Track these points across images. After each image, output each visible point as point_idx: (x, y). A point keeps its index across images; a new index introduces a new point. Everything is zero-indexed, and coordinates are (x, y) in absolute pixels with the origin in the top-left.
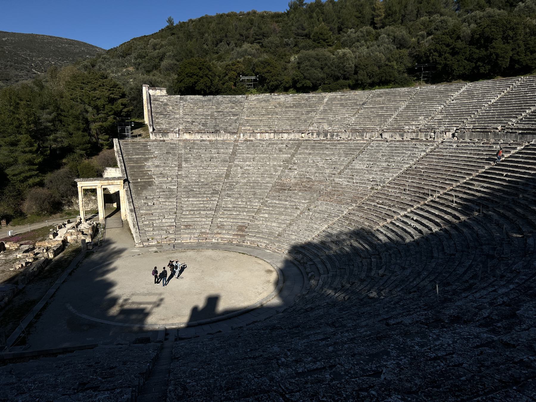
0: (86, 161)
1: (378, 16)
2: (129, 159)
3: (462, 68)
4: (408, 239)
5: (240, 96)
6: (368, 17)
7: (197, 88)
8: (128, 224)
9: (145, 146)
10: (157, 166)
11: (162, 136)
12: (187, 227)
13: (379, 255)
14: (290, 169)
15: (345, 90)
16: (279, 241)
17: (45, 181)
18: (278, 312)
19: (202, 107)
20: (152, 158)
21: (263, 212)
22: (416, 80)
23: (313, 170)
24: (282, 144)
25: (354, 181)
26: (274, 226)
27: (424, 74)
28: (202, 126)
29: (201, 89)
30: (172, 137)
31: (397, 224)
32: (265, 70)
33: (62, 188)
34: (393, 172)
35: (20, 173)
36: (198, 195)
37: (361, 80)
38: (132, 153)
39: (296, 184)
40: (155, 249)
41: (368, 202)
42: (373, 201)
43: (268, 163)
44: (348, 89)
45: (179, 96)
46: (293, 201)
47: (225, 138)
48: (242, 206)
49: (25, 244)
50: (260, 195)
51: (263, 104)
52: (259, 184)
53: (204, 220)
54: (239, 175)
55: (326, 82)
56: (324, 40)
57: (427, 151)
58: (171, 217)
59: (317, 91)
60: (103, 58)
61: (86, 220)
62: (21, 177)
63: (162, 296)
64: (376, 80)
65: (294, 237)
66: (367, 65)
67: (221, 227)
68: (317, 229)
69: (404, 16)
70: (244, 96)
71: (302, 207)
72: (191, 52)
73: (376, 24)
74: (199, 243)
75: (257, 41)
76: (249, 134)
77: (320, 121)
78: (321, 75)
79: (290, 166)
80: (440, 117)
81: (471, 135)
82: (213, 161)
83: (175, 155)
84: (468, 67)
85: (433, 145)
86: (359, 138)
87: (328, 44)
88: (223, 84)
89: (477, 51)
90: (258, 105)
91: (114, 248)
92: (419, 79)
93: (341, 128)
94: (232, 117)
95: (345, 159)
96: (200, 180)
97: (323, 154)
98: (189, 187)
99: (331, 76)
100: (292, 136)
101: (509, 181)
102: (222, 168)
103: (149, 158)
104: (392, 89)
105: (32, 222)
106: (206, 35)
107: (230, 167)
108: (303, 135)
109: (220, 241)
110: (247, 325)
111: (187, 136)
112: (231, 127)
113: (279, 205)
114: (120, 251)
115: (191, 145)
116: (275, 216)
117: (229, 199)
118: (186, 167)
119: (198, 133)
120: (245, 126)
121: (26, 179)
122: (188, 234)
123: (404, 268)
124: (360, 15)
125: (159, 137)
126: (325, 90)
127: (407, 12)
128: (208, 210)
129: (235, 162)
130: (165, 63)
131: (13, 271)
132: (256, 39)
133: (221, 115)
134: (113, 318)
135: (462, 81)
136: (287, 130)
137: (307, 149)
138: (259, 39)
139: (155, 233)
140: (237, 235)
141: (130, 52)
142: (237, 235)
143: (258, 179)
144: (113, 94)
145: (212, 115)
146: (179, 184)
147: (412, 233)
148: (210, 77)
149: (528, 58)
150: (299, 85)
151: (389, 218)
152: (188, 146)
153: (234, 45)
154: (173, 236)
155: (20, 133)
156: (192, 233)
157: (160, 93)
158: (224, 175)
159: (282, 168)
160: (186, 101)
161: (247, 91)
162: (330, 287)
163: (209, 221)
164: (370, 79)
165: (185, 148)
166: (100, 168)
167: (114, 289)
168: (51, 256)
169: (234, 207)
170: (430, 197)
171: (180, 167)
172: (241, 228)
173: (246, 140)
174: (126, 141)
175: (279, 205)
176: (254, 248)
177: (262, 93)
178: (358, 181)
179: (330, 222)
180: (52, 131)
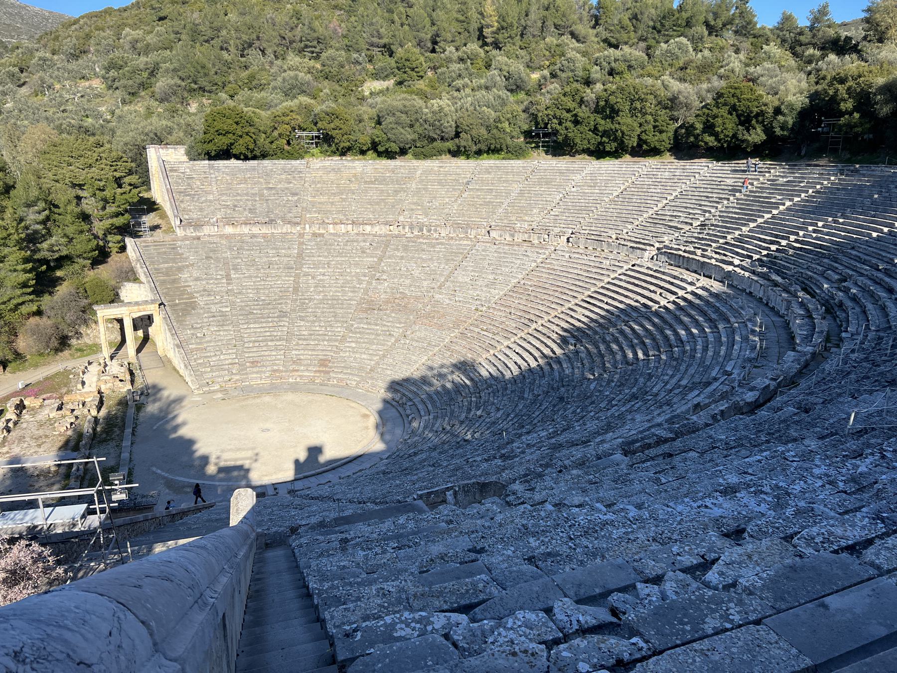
0: (91, 274)
1: (488, 26)
2: (156, 269)
3: (586, 142)
4: (508, 375)
5: (298, 162)
6: (474, 26)
7: (234, 151)
8: (170, 361)
9: (173, 248)
10: (197, 279)
11: (195, 231)
12: (254, 363)
13: (479, 393)
14: (378, 279)
15: (443, 156)
16: (372, 378)
17: (43, 308)
18: (382, 459)
19: (245, 181)
20: (187, 266)
21: (348, 340)
22: (535, 147)
23: (408, 282)
24: (364, 241)
25: (457, 299)
26: (364, 359)
27: (543, 142)
28: (249, 213)
29: (241, 153)
30: (207, 230)
31: (500, 357)
32: (332, 125)
33: (70, 317)
34: (499, 289)
35: (9, 301)
36: (260, 320)
37: (465, 147)
38: (158, 261)
39: (387, 302)
40: (220, 395)
41: (472, 328)
42: (477, 327)
43: (349, 271)
44: (448, 156)
45: (207, 162)
46: (385, 325)
47: (284, 230)
48: (321, 332)
49: (48, 398)
50: (343, 317)
51: (332, 176)
52: (340, 301)
53: (274, 353)
54: (312, 289)
55: (418, 145)
56: (413, 70)
57: (539, 261)
58: (230, 351)
59: (407, 156)
60: (40, 59)
61: (112, 358)
62: (11, 305)
63: (256, 451)
64: (483, 147)
65: (389, 372)
66: (471, 124)
67: (297, 362)
68: (416, 362)
69: (525, 28)
70: (303, 162)
71: (397, 333)
72: (203, 67)
73: (486, 38)
74: (272, 384)
75: (308, 50)
76: (318, 226)
77: (414, 207)
78: (410, 137)
79: (378, 275)
80: (556, 211)
81: (586, 243)
82: (273, 268)
83: (217, 260)
84: (593, 141)
85: (545, 254)
86: (462, 236)
87: (418, 74)
88: (272, 142)
89: (603, 122)
90: (325, 178)
91: (168, 397)
92: (537, 147)
93: (439, 220)
94: (290, 198)
95: (446, 267)
96: (259, 298)
97: (419, 258)
98: (247, 308)
99: (425, 137)
100: (376, 229)
101: (607, 311)
102: (287, 278)
103: (183, 266)
104: (504, 162)
105: (36, 366)
106: (224, 32)
107: (297, 276)
108: (391, 227)
109: (298, 380)
110: (354, 474)
111: (229, 230)
112: (290, 215)
113: (368, 331)
114: (179, 400)
115: (239, 244)
116: (364, 345)
117: (302, 323)
118: (238, 278)
119: (246, 224)
120: (310, 213)
121: (17, 306)
122: (257, 373)
123: (498, 409)
124: (462, 18)
125: (190, 232)
126: (417, 156)
127: (529, 23)
128: (277, 340)
129: (304, 270)
130: (162, 83)
131: (60, 435)
132: (306, 46)
133: (274, 194)
134: (212, 477)
135: (587, 157)
136: (370, 219)
137: (398, 250)
138: (311, 47)
139: (214, 374)
140: (319, 371)
141: (87, 47)
142: (319, 371)
143: (338, 294)
144: (116, 170)
145: (262, 195)
146: (233, 304)
147: (512, 368)
148: (254, 137)
149: (656, 138)
150: (380, 149)
151: (492, 349)
152: (235, 246)
153: (272, 56)
154: (238, 377)
155: (6, 246)
156: (262, 371)
157: (176, 155)
158: (291, 289)
159: (367, 278)
160: (218, 170)
161: (306, 152)
162: (431, 431)
163: (280, 355)
164: (476, 145)
165: (231, 249)
166: (113, 283)
167: (195, 447)
168: (94, 412)
169: (311, 335)
170: (535, 324)
171: (228, 277)
172: (323, 363)
173: (315, 235)
174: (145, 242)
175: (368, 331)
176: (343, 387)
177: (329, 156)
178: (461, 299)
179: (431, 353)
180: (43, 236)
